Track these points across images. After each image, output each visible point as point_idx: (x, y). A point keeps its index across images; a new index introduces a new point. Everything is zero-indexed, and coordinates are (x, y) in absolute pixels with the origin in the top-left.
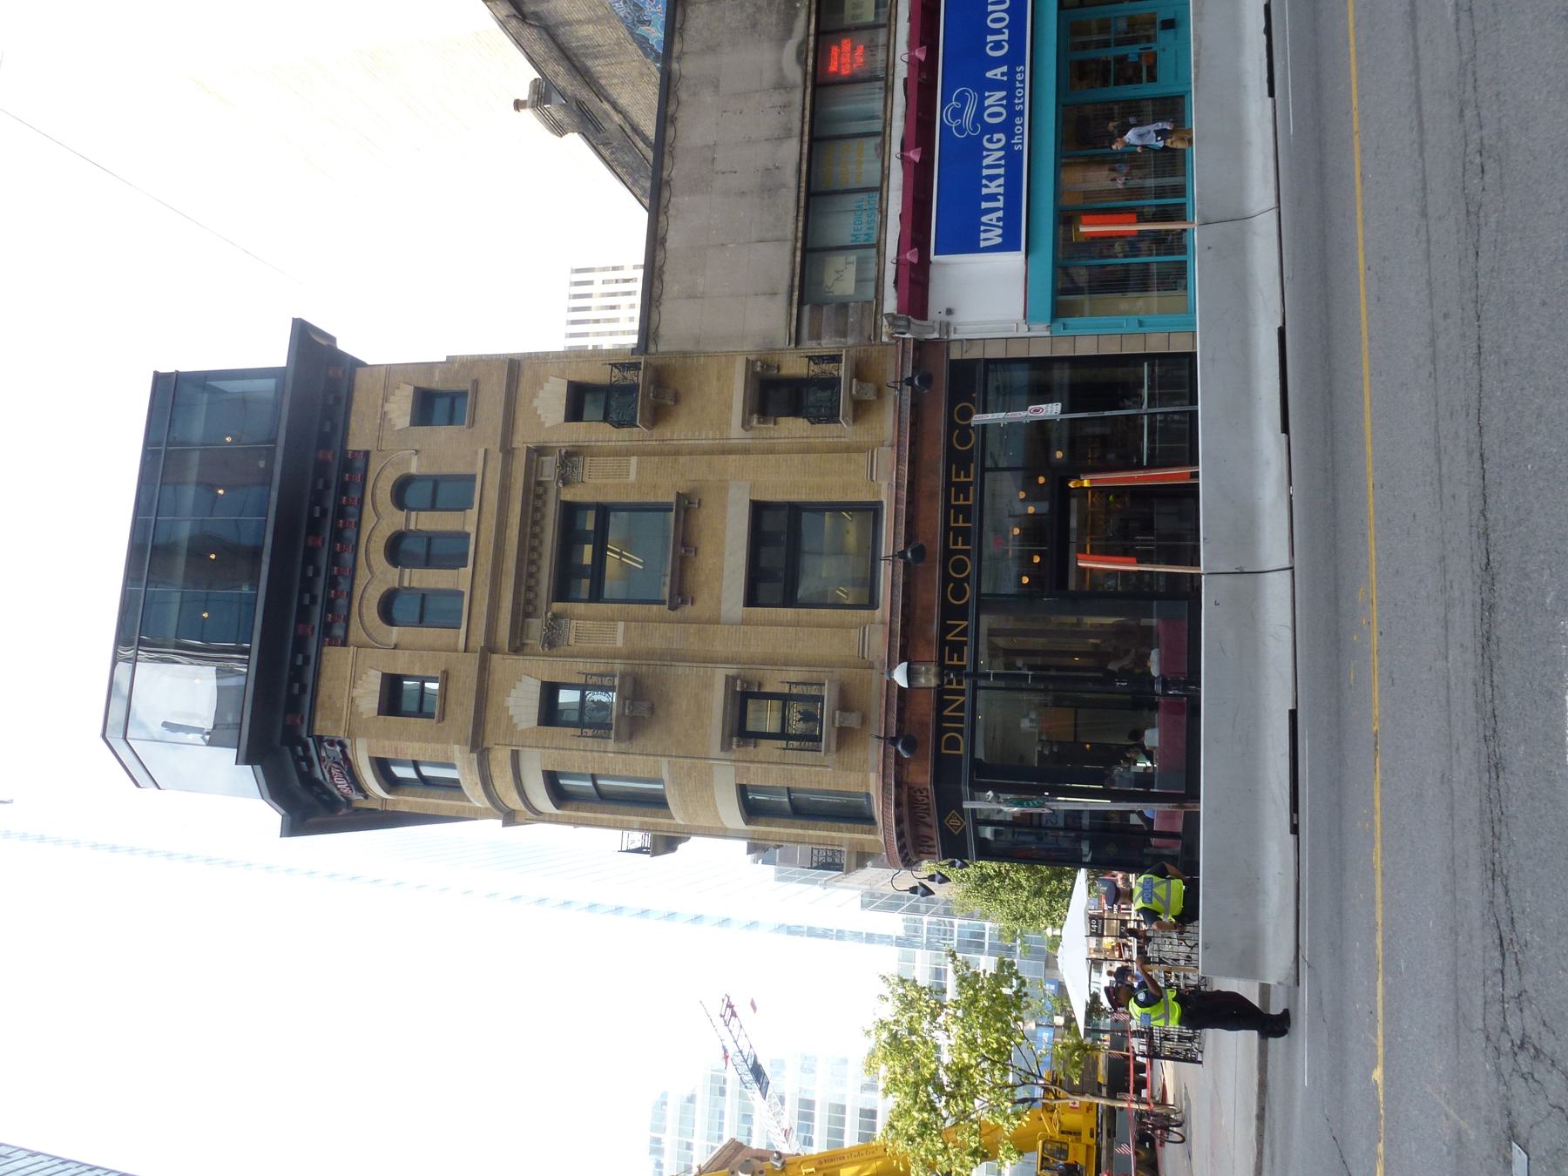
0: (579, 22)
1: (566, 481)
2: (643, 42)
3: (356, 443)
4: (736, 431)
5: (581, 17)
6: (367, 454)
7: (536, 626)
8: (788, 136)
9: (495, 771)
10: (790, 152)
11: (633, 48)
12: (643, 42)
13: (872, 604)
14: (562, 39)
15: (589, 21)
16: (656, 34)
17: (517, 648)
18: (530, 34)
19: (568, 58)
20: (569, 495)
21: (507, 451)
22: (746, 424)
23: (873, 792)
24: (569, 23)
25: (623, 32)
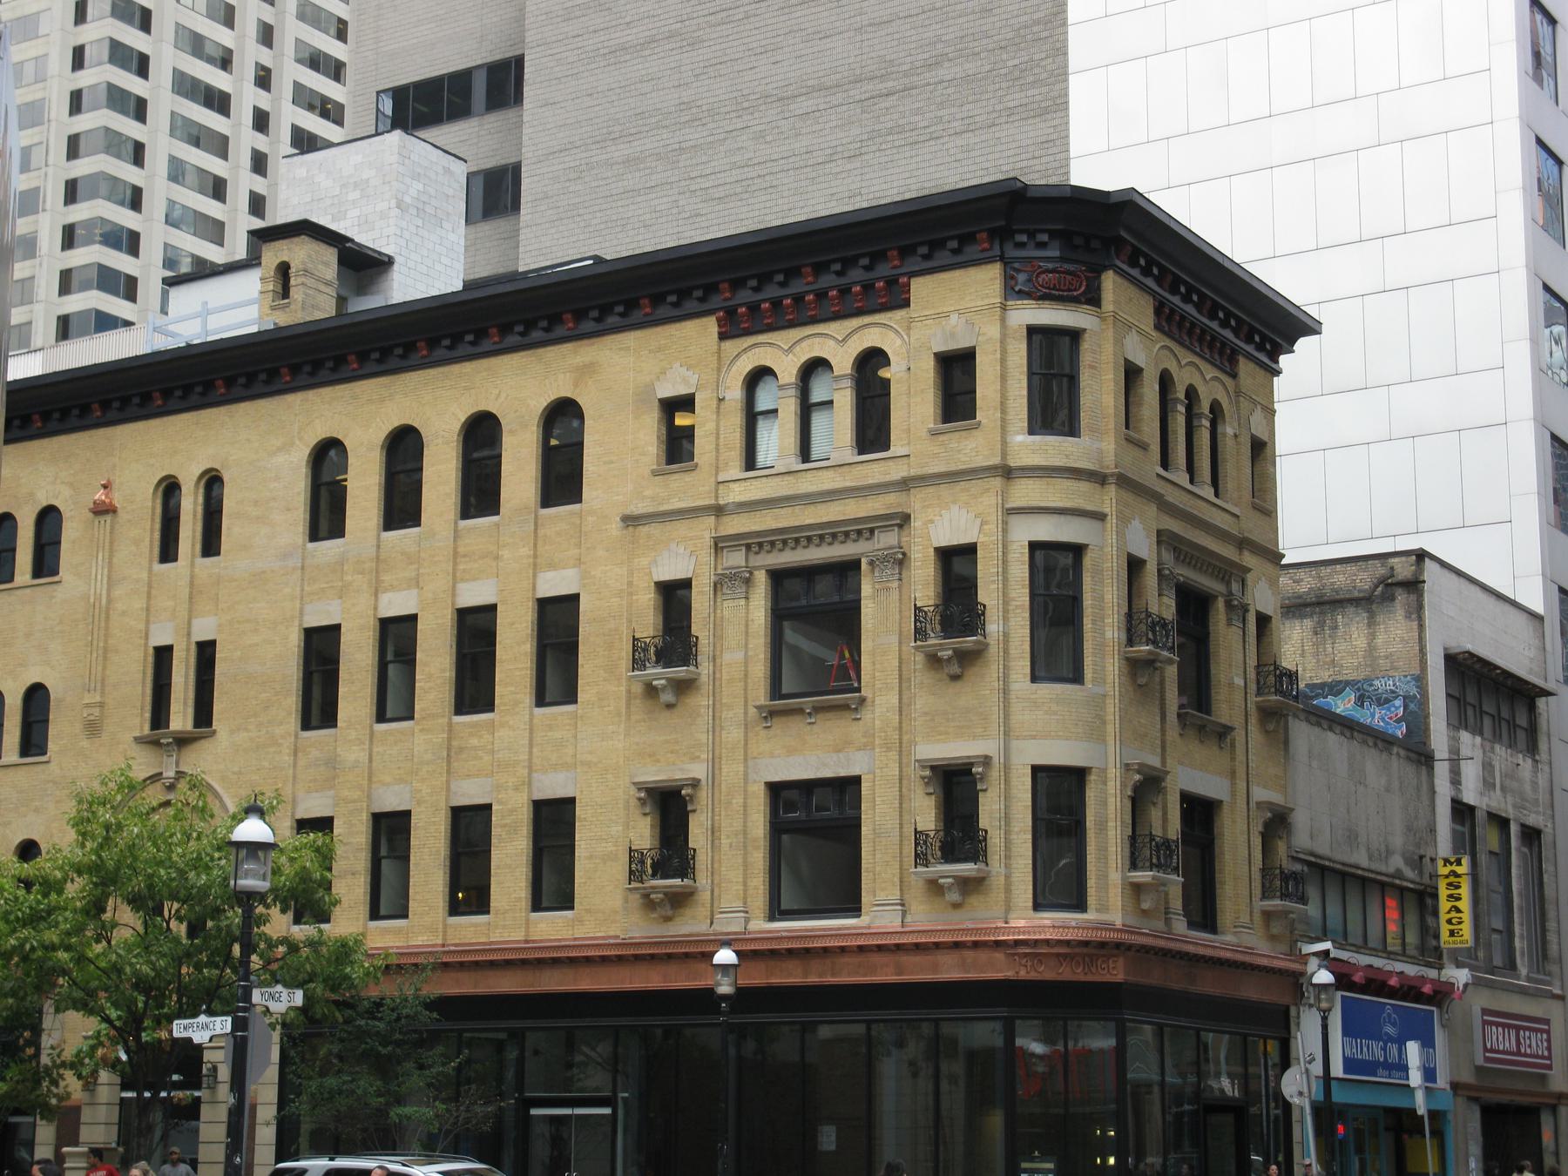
0: (1372, 636)
1: (1228, 604)
2: (1335, 688)
3: (1244, 367)
4: (1260, 794)
5: (1380, 640)
6: (1234, 376)
7: (1168, 557)
8: (1370, 859)
9: (1084, 486)
10: (1360, 858)
11: (1326, 676)
12: (1335, 688)
13: (1192, 925)
14: (1351, 610)
15: (1371, 649)
16: (1343, 705)
17: (1164, 538)
18: (1363, 580)
19: (1319, 604)
20: (1220, 604)
21: (1243, 543)
22: (1270, 806)
23: (1090, 916)
24: (1371, 623)
25: (1349, 674)
